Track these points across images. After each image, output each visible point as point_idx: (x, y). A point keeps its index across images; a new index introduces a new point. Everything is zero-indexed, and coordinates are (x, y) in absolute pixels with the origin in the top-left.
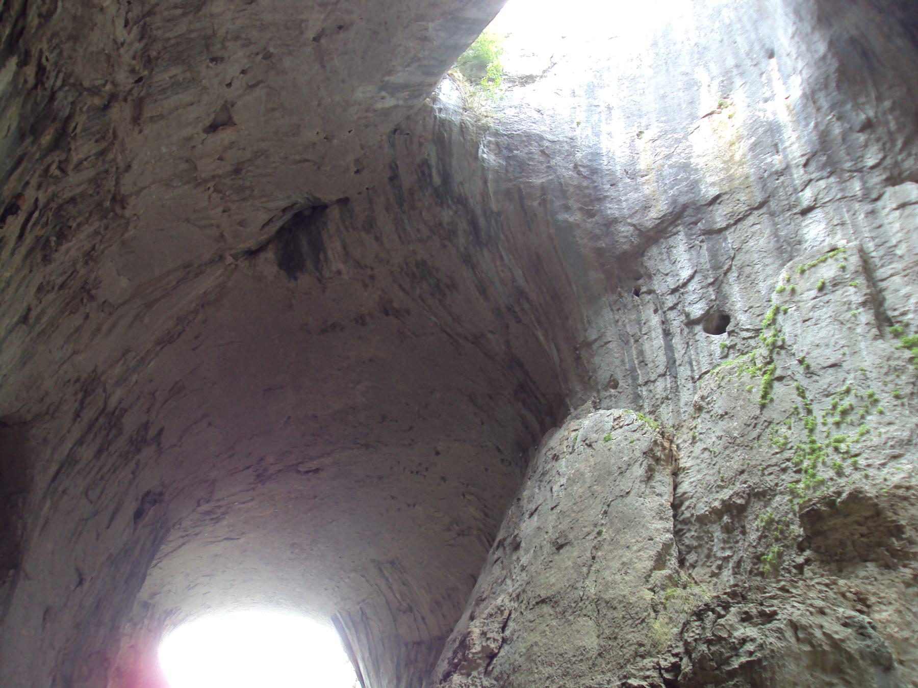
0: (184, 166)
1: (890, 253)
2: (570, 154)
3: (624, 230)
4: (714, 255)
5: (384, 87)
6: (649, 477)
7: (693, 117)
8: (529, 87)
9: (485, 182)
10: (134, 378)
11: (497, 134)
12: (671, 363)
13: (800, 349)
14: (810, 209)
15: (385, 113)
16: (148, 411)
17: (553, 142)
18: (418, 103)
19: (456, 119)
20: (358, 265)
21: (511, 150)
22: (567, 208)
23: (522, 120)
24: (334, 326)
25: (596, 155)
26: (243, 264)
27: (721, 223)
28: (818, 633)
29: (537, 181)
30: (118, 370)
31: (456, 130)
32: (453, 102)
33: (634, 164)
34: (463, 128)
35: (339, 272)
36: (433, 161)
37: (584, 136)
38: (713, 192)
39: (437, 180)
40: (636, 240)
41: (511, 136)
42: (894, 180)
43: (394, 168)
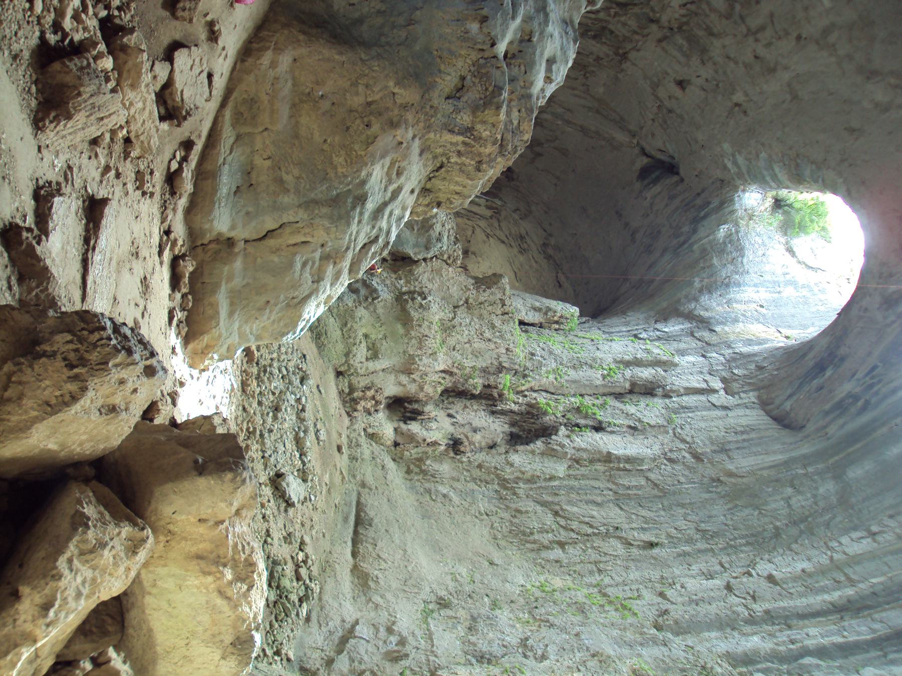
0: (655, 80)
1: (673, 376)
2: (737, 273)
3: (693, 305)
4: (677, 336)
5: (733, 156)
6: (535, 309)
7: (777, 326)
8: (787, 254)
9: (708, 236)
10: (560, 122)
11: (737, 232)
12: (612, 333)
13: (609, 343)
14: (703, 356)
15: (725, 168)
16: (548, 141)
17: (742, 262)
18: (738, 182)
19: (737, 206)
20: (652, 204)
21: (730, 243)
22: (702, 281)
23: (753, 245)
24: (621, 216)
25: (739, 285)
26: (637, 151)
27: (696, 335)
28: (434, 221)
29: (715, 261)
30: (560, 110)
31: (731, 209)
32: (747, 202)
33: (736, 302)
34: (733, 212)
35: (646, 199)
36: (711, 206)
37: (752, 278)
38: (718, 329)
39: (702, 214)
40: (686, 311)
41: (738, 240)
42: (724, 380)
43: (703, 191)
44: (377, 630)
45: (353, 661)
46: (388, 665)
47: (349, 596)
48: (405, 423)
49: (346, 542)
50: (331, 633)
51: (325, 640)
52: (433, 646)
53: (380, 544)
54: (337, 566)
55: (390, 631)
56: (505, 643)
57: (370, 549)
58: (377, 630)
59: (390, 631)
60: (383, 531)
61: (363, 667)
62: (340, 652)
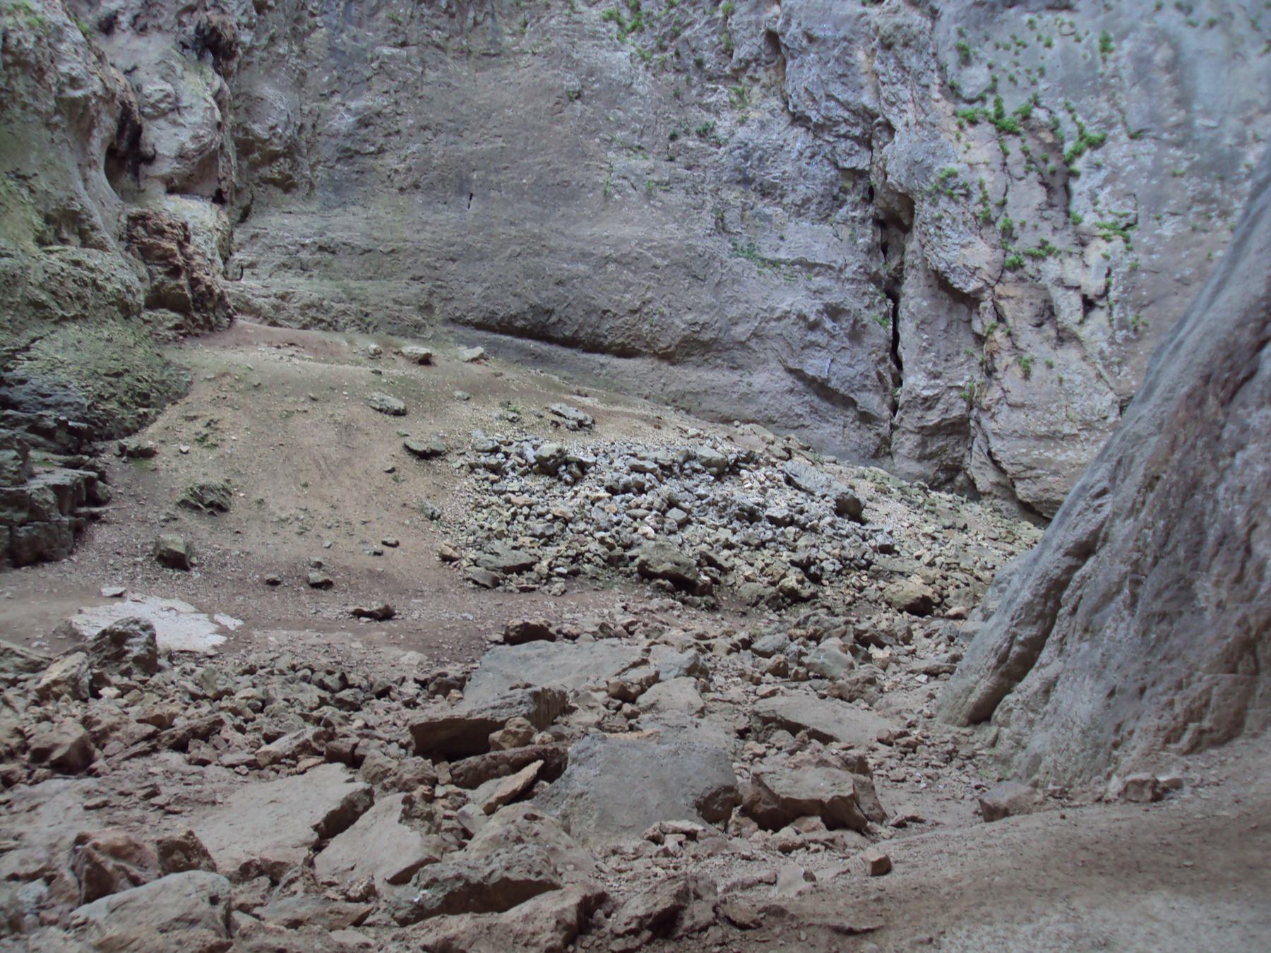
44: (813, 344)
45: (865, 386)
46: (868, 340)
47: (735, 377)
48: (150, 160)
49: (602, 366)
50: (814, 411)
51: (828, 421)
52: (830, 267)
53: (602, 302)
54: (673, 388)
55: (814, 326)
56: (808, 153)
57: (619, 322)
58: (813, 344)
59: (814, 326)
60: (561, 290)
61: (873, 374)
62: (853, 403)
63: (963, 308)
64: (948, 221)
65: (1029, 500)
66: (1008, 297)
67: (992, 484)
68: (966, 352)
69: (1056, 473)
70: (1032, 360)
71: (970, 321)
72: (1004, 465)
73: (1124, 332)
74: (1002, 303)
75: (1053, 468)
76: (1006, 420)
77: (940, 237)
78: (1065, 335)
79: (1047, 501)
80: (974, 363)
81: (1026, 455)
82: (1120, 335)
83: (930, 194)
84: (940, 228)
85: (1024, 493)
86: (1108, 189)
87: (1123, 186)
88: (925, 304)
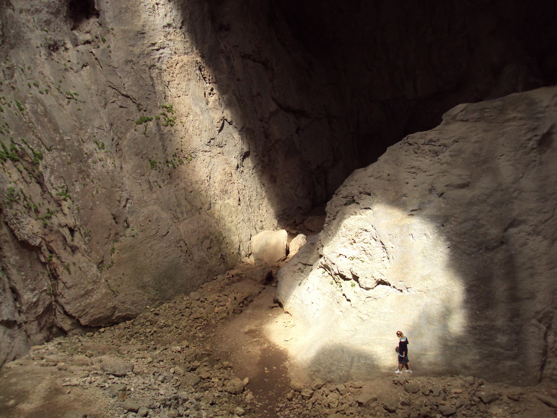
63: (35, 254)
64: (20, 214)
65: (87, 324)
66: (52, 241)
67: (70, 325)
68: (41, 273)
69: (93, 307)
70: (69, 264)
71: (38, 258)
72: (74, 315)
73: (87, 238)
74: (51, 244)
75: (91, 306)
76: (68, 294)
77: (19, 223)
78: (74, 248)
79: (94, 320)
80: (46, 277)
81: (80, 306)
82: (86, 239)
83: (8, 203)
84: (17, 219)
85: (84, 322)
86: (53, 177)
87: (57, 174)
88: (18, 258)
